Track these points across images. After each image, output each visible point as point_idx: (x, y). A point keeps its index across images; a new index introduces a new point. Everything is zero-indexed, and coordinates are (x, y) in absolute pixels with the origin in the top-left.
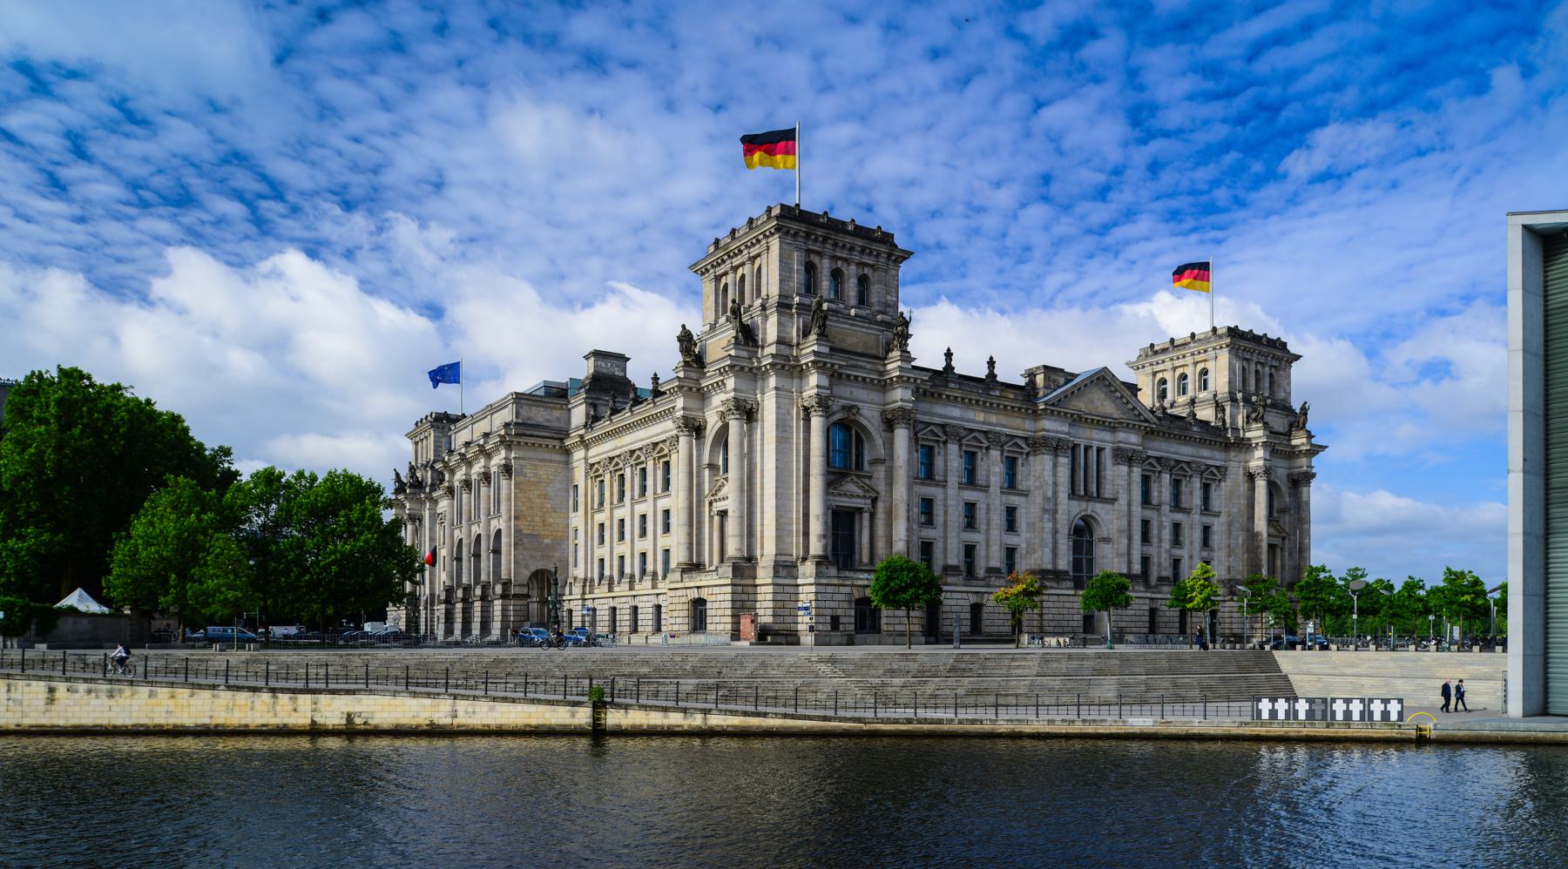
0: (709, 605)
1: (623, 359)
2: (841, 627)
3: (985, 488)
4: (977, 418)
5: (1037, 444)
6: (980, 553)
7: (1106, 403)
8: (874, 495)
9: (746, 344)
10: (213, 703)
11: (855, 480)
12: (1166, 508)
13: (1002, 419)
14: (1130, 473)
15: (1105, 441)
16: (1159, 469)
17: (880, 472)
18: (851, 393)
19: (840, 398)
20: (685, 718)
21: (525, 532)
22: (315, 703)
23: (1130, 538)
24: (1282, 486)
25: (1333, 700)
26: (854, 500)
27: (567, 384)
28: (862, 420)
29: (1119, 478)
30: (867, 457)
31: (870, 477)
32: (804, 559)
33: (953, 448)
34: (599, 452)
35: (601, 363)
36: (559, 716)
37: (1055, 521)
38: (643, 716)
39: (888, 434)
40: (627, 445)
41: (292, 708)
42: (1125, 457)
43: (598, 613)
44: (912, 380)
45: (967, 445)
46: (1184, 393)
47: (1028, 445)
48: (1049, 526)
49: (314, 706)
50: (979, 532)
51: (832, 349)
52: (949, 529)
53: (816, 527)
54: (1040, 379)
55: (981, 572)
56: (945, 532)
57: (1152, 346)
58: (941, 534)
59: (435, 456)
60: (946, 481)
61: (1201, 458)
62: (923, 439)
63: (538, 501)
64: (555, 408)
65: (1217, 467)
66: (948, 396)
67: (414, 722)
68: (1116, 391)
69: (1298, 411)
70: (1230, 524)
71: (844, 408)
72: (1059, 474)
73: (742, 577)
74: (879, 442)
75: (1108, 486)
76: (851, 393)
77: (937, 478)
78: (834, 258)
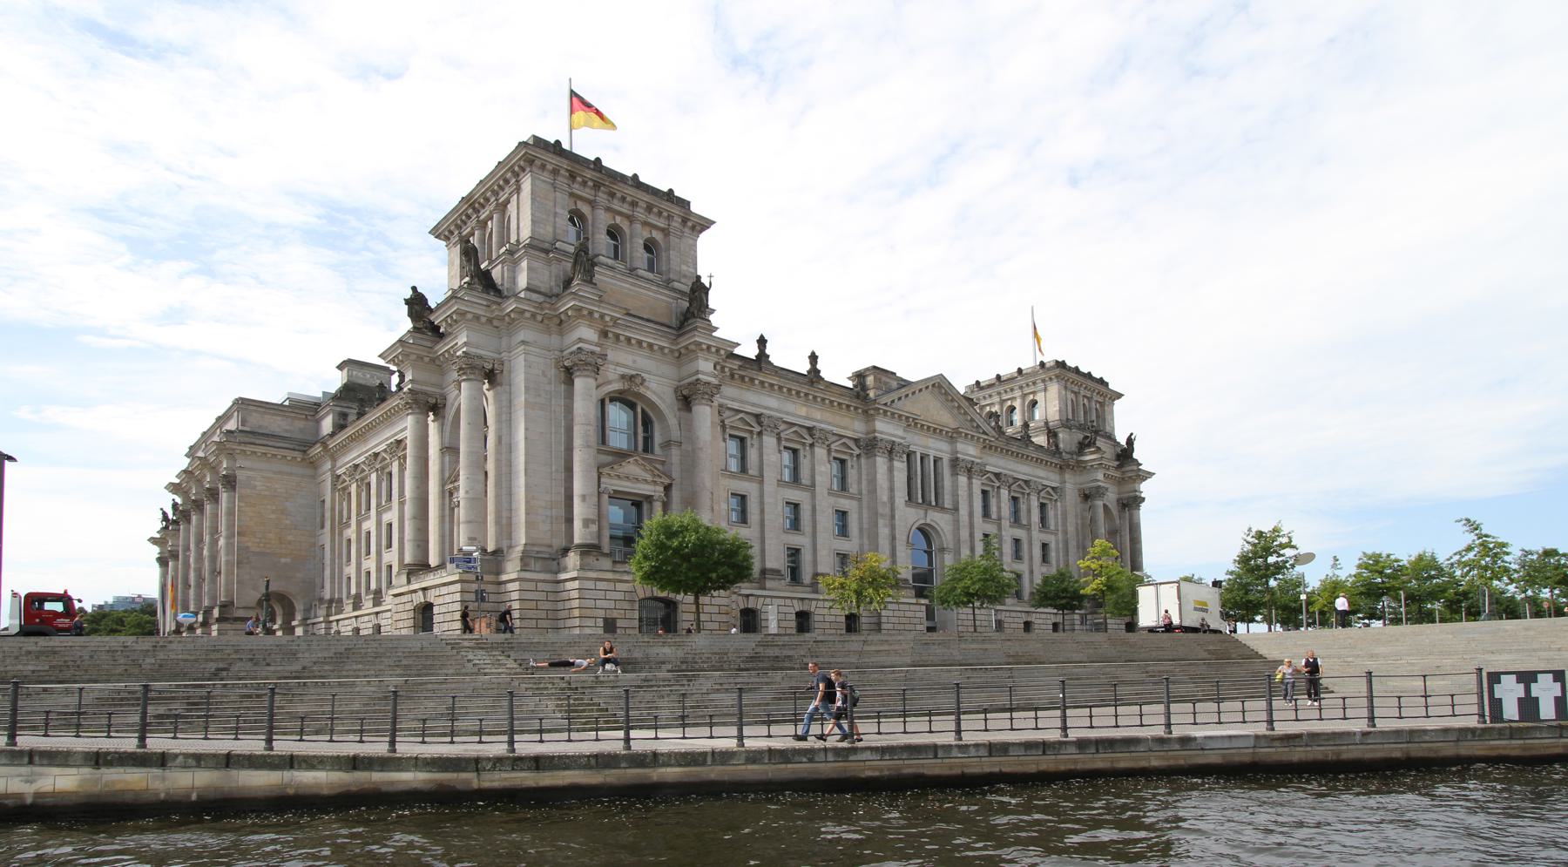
4: (798, 411)
5: (869, 446)
13: (828, 416)
14: (970, 484)
15: (941, 451)
19: (617, 364)
28: (649, 394)
29: (965, 490)
44: (713, 350)
45: (787, 440)
47: (859, 447)
62: (732, 427)
65: (1053, 488)
66: (762, 383)
71: (623, 377)
72: (895, 479)
74: (672, 421)
76: (634, 362)
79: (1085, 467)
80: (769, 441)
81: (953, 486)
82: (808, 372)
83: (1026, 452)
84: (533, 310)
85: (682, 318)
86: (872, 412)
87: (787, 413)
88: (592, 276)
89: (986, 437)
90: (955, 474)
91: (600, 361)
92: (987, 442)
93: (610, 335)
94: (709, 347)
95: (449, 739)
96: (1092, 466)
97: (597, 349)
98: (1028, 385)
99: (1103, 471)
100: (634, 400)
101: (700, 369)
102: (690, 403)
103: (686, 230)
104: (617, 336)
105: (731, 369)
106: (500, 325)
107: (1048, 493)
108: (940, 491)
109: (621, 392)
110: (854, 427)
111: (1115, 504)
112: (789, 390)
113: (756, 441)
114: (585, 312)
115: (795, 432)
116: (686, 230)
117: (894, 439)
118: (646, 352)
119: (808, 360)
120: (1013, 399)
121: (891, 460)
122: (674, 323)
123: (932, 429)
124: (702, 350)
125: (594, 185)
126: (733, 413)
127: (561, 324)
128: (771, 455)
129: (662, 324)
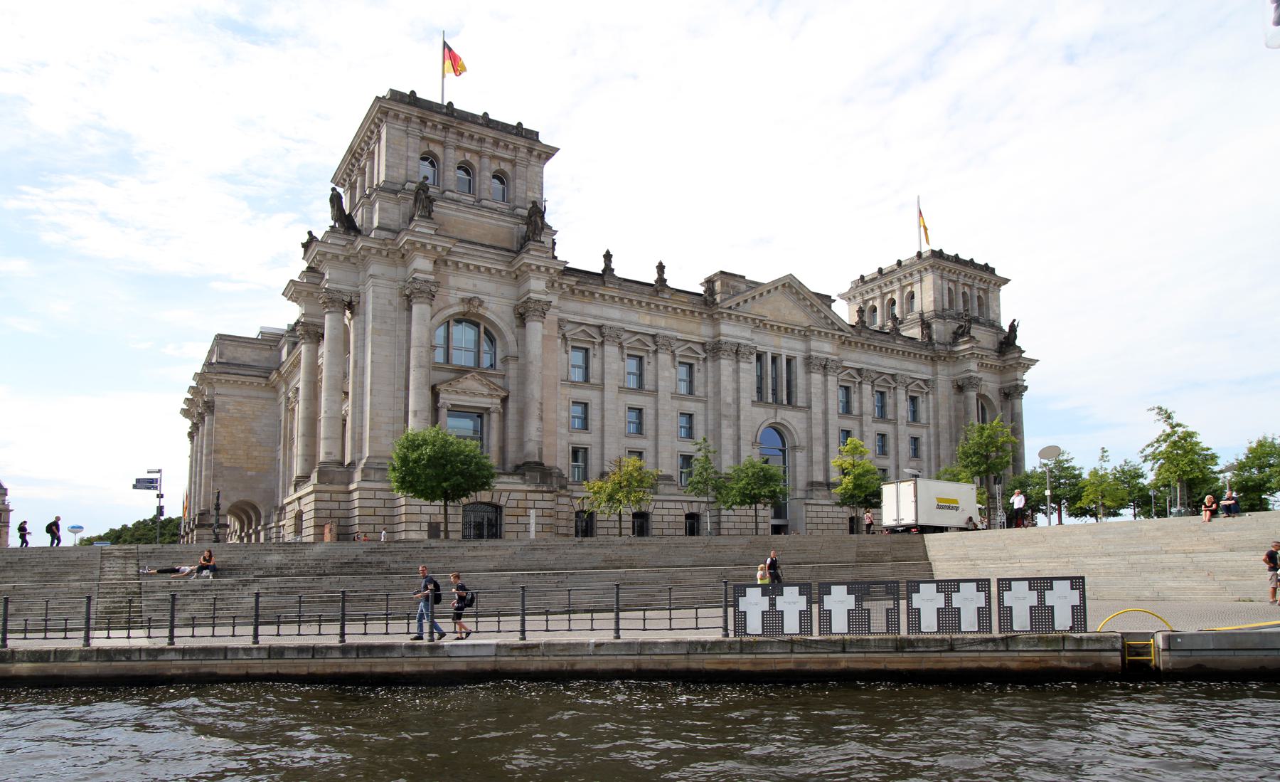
4: (641, 320)
5: (714, 349)
7: (794, 312)
8: (503, 394)
11: (478, 377)
12: (868, 419)
13: (673, 323)
14: (825, 382)
15: (795, 350)
16: (859, 380)
19: (458, 289)
21: (225, 465)
24: (993, 400)
26: (477, 399)
28: (488, 315)
29: (813, 385)
30: (499, 355)
39: (521, 330)
44: (543, 269)
45: (629, 348)
47: (705, 351)
57: (862, 277)
62: (573, 340)
63: (242, 435)
65: (925, 381)
66: (603, 296)
71: (463, 300)
74: (510, 338)
76: (475, 285)
77: (592, 381)
79: (957, 358)
80: (611, 350)
81: (807, 385)
82: (656, 282)
83: (891, 346)
85: (523, 241)
86: (716, 316)
87: (630, 323)
88: (430, 212)
89: (841, 333)
90: (809, 372)
91: (433, 289)
92: (843, 338)
93: (449, 263)
94: (538, 267)
95: (42, 635)
96: (964, 356)
97: (432, 278)
98: (905, 277)
99: (978, 361)
100: (478, 321)
101: (532, 288)
102: (524, 319)
103: (533, 159)
104: (456, 263)
105: (568, 285)
106: (356, 261)
109: (464, 314)
110: (701, 331)
111: (996, 394)
112: (631, 301)
113: (598, 352)
114: (418, 245)
115: (638, 340)
116: (533, 159)
117: (740, 341)
118: (486, 276)
119: (656, 270)
120: (893, 292)
122: (515, 247)
123: (782, 329)
124: (532, 270)
125: (444, 128)
126: (574, 326)
127: (403, 258)
128: (613, 364)
129: (501, 249)
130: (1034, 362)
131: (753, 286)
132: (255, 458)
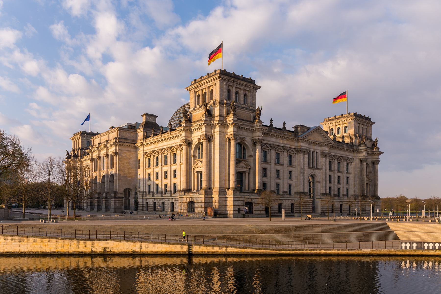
0: (195, 204)
1: (155, 116)
2: (241, 211)
3: (283, 165)
4: (280, 142)
6: (281, 186)
8: (250, 167)
9: (209, 116)
10: (56, 244)
11: (244, 162)
14: (326, 160)
15: (318, 150)
17: (251, 159)
18: (243, 133)
20: (220, 249)
21: (122, 175)
22: (93, 244)
23: (326, 181)
25: (424, 243)
26: (243, 169)
27: (135, 124)
28: (246, 142)
30: (247, 155)
31: (248, 161)
32: (229, 189)
33: (273, 152)
34: (149, 148)
35: (148, 118)
36: (177, 248)
37: (304, 176)
38: (206, 249)
39: (254, 147)
40: (160, 147)
41: (85, 246)
42: (325, 155)
43: (148, 204)
44: (262, 130)
46: (339, 134)
47: (295, 151)
48: (302, 177)
49: (92, 245)
50: (281, 179)
51: (238, 119)
52: (272, 178)
53: (232, 178)
54: (299, 129)
55: (281, 193)
56: (271, 179)
58: (269, 180)
59: (82, 146)
60: (271, 163)
61: (346, 155)
62: (264, 149)
63: (126, 165)
64: (133, 133)
65: (351, 158)
66: (272, 135)
67: (127, 251)
68: (322, 134)
69: (374, 141)
70: (355, 177)
71: (240, 138)
73: (208, 195)
75: (319, 165)
76: (243, 133)
77: (268, 161)
78: (237, 88)
84: (222, 123)
89: (331, 145)
102: (256, 145)
107: (349, 160)
108: (318, 163)
121: (304, 155)
130: (382, 153)
131: (308, 129)
132: (130, 173)
